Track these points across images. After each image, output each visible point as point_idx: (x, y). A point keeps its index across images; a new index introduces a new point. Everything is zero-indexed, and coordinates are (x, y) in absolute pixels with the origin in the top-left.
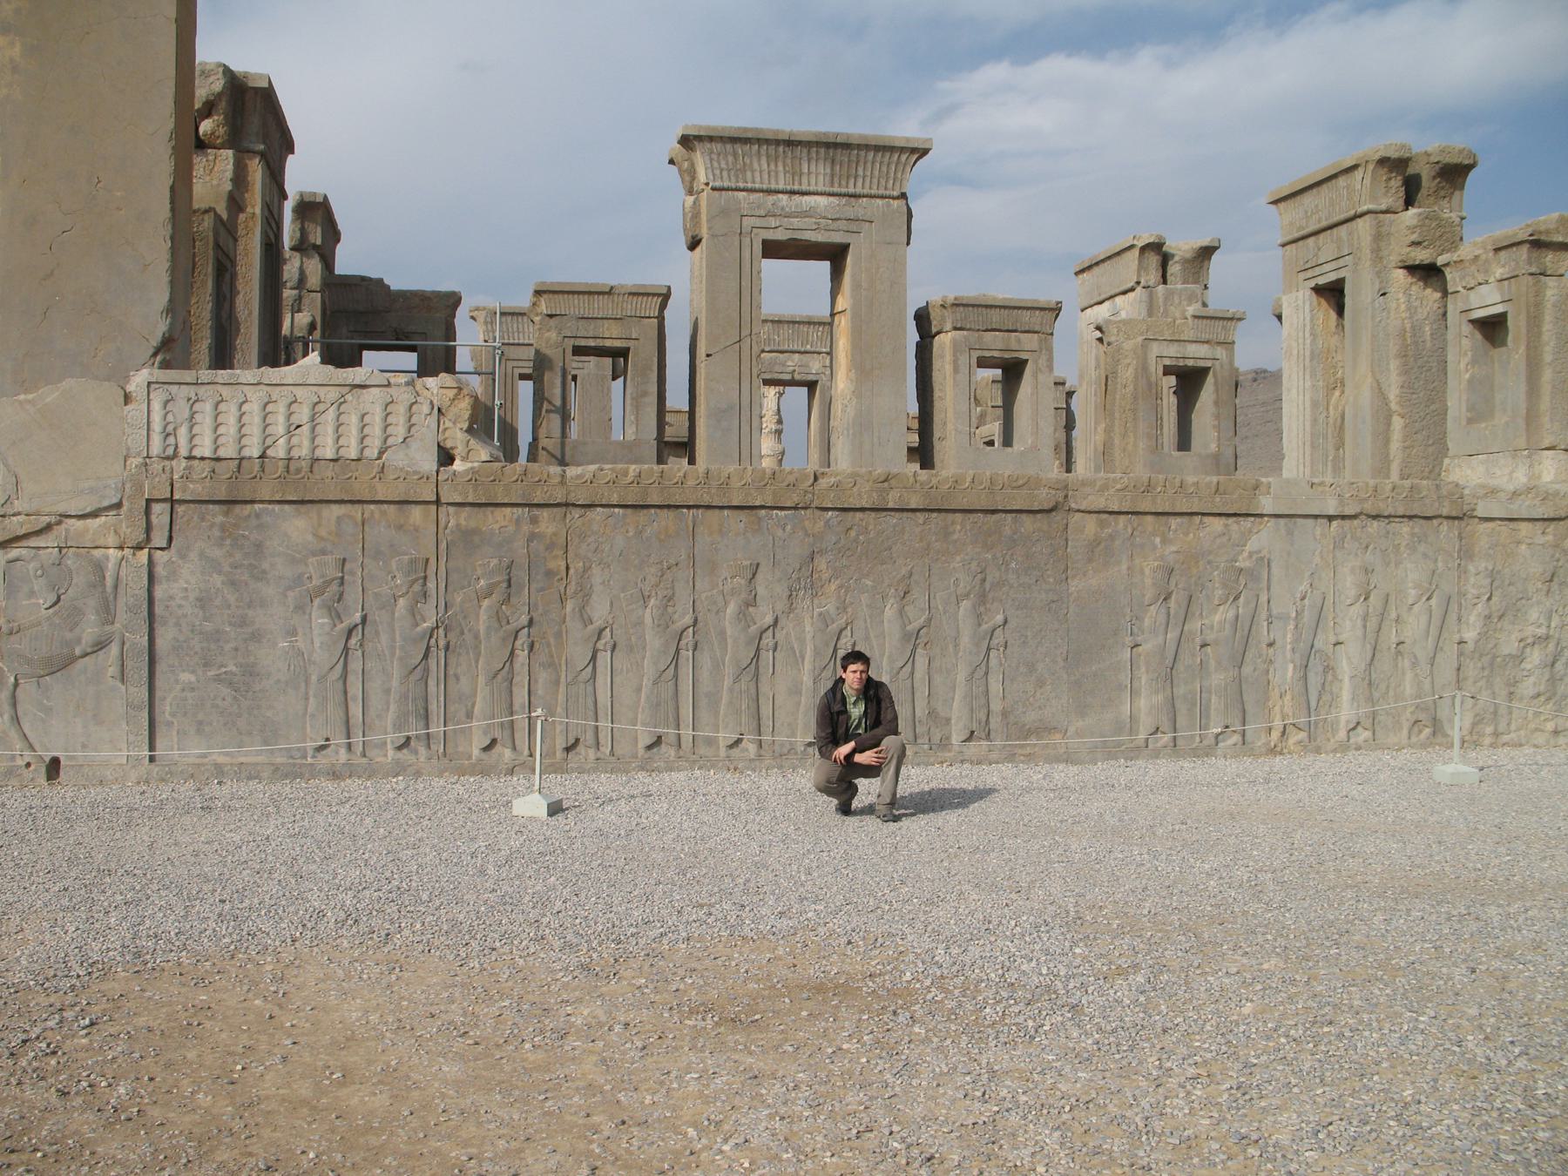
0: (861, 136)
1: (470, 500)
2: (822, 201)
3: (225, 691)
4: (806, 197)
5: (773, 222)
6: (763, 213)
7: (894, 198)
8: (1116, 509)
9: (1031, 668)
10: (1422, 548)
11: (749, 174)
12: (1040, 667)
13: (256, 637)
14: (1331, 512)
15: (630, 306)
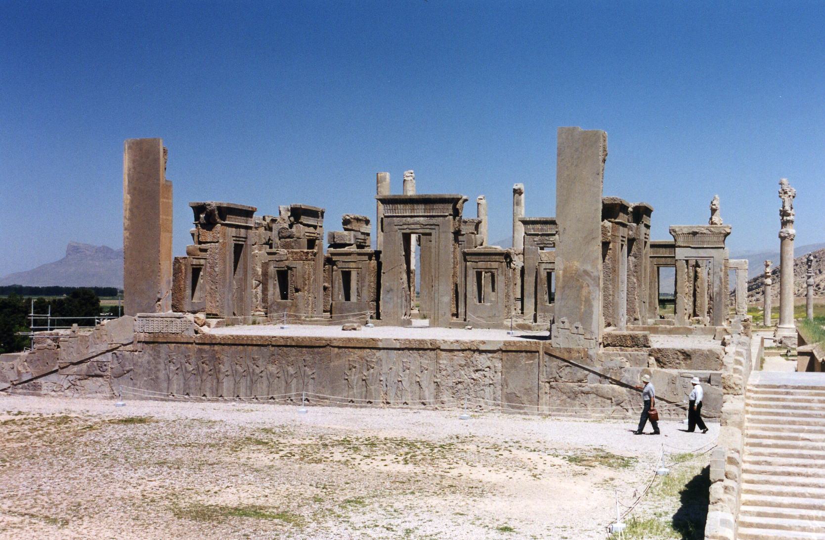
0: (434, 195)
1: (200, 342)
2: (422, 219)
3: (153, 382)
4: (415, 218)
5: (405, 227)
6: (401, 224)
7: (446, 216)
8: (341, 345)
9: (321, 383)
10: (425, 356)
11: (397, 211)
12: (323, 383)
13: (159, 370)
14: (398, 347)
15: (359, 258)
